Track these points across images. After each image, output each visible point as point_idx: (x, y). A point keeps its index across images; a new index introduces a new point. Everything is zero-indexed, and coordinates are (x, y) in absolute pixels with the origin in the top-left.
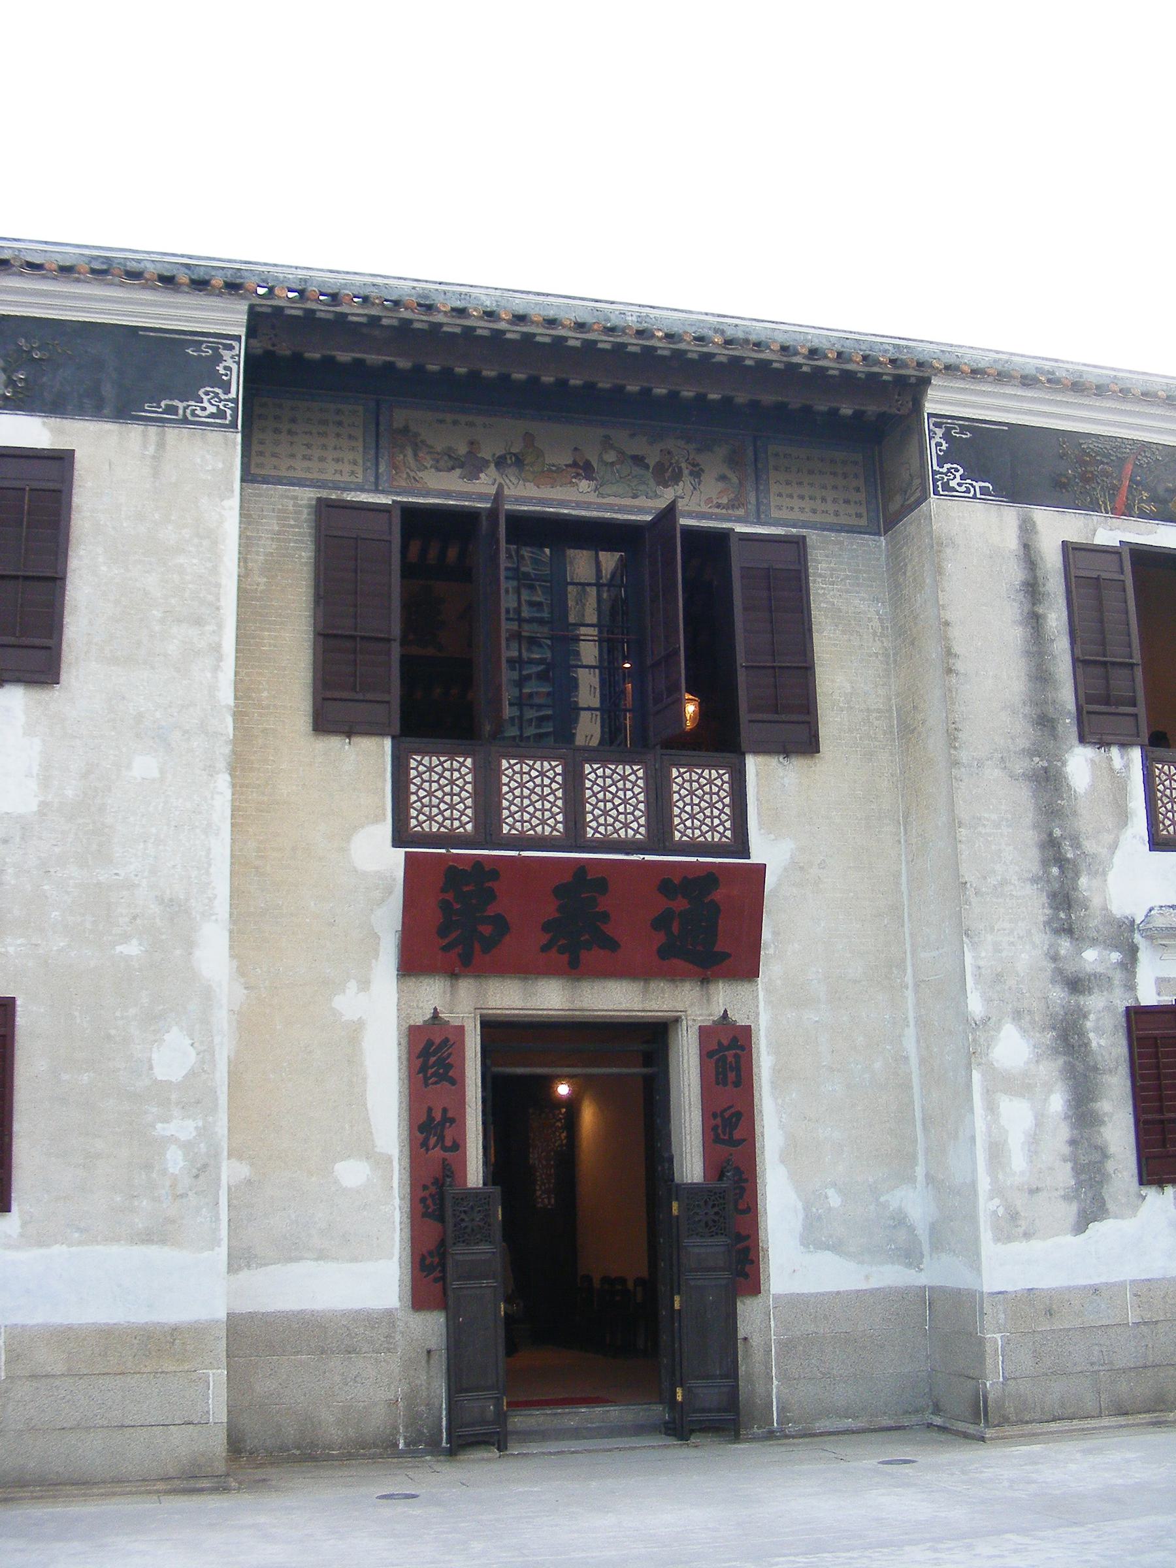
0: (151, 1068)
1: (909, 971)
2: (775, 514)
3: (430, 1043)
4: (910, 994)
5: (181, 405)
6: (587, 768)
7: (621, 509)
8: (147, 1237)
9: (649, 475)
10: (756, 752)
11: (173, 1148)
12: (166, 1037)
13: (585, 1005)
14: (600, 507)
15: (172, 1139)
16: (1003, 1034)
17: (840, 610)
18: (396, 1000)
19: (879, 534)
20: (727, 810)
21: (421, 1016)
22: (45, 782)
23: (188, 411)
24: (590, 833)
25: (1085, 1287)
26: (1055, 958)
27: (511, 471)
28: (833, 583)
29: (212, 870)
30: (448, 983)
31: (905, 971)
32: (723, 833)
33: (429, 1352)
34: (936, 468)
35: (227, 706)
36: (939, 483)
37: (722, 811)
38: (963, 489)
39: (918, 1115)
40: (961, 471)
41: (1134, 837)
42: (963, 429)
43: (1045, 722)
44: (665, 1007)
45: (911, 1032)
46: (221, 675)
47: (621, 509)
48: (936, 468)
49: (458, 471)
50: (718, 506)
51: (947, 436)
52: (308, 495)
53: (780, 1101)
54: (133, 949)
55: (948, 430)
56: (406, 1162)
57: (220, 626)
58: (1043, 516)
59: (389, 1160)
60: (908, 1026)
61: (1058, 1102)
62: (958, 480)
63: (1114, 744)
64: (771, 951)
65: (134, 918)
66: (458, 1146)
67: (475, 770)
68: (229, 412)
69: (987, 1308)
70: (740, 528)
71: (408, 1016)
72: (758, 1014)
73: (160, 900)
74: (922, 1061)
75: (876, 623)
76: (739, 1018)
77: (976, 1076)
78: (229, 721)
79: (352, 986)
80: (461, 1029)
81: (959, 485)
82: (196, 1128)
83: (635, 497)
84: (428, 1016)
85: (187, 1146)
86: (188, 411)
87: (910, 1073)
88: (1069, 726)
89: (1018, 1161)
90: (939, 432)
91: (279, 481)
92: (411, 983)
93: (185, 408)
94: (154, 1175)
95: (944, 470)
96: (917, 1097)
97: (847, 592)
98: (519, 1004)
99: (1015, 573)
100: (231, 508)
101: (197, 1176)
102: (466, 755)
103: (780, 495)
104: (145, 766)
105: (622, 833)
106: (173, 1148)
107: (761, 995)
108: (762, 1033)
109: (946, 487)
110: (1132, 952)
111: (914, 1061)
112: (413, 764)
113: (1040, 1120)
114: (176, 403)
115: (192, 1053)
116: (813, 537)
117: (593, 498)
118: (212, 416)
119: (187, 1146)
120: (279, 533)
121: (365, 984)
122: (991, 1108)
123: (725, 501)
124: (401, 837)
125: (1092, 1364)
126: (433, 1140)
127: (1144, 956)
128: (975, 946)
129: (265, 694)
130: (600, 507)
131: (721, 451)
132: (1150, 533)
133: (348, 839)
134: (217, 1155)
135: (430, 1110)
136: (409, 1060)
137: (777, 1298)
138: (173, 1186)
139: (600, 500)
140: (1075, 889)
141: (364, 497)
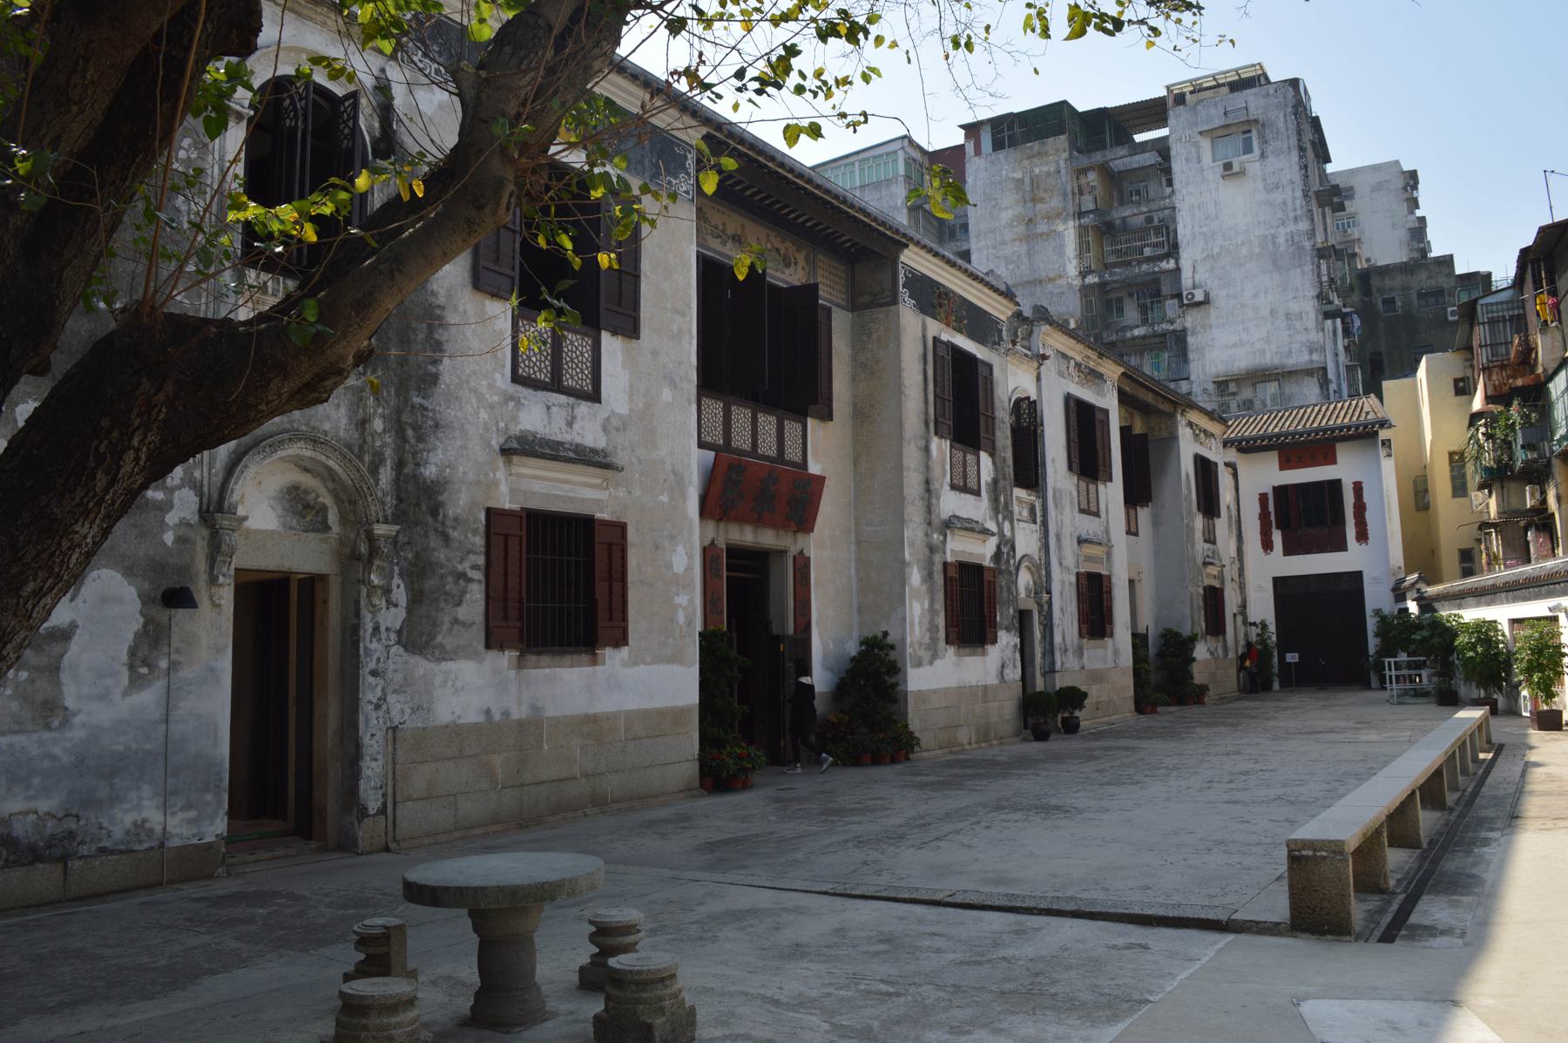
9: (781, 260)
10: (812, 417)
15: (680, 605)
21: (707, 543)
26: (927, 535)
27: (737, 244)
32: (798, 458)
42: (910, 272)
45: (853, 565)
51: (905, 274)
58: (929, 321)
85: (685, 609)
98: (738, 538)
99: (920, 350)
110: (945, 536)
116: (834, 308)
119: (685, 609)
122: (911, 605)
124: (702, 445)
127: (949, 538)
131: (803, 253)
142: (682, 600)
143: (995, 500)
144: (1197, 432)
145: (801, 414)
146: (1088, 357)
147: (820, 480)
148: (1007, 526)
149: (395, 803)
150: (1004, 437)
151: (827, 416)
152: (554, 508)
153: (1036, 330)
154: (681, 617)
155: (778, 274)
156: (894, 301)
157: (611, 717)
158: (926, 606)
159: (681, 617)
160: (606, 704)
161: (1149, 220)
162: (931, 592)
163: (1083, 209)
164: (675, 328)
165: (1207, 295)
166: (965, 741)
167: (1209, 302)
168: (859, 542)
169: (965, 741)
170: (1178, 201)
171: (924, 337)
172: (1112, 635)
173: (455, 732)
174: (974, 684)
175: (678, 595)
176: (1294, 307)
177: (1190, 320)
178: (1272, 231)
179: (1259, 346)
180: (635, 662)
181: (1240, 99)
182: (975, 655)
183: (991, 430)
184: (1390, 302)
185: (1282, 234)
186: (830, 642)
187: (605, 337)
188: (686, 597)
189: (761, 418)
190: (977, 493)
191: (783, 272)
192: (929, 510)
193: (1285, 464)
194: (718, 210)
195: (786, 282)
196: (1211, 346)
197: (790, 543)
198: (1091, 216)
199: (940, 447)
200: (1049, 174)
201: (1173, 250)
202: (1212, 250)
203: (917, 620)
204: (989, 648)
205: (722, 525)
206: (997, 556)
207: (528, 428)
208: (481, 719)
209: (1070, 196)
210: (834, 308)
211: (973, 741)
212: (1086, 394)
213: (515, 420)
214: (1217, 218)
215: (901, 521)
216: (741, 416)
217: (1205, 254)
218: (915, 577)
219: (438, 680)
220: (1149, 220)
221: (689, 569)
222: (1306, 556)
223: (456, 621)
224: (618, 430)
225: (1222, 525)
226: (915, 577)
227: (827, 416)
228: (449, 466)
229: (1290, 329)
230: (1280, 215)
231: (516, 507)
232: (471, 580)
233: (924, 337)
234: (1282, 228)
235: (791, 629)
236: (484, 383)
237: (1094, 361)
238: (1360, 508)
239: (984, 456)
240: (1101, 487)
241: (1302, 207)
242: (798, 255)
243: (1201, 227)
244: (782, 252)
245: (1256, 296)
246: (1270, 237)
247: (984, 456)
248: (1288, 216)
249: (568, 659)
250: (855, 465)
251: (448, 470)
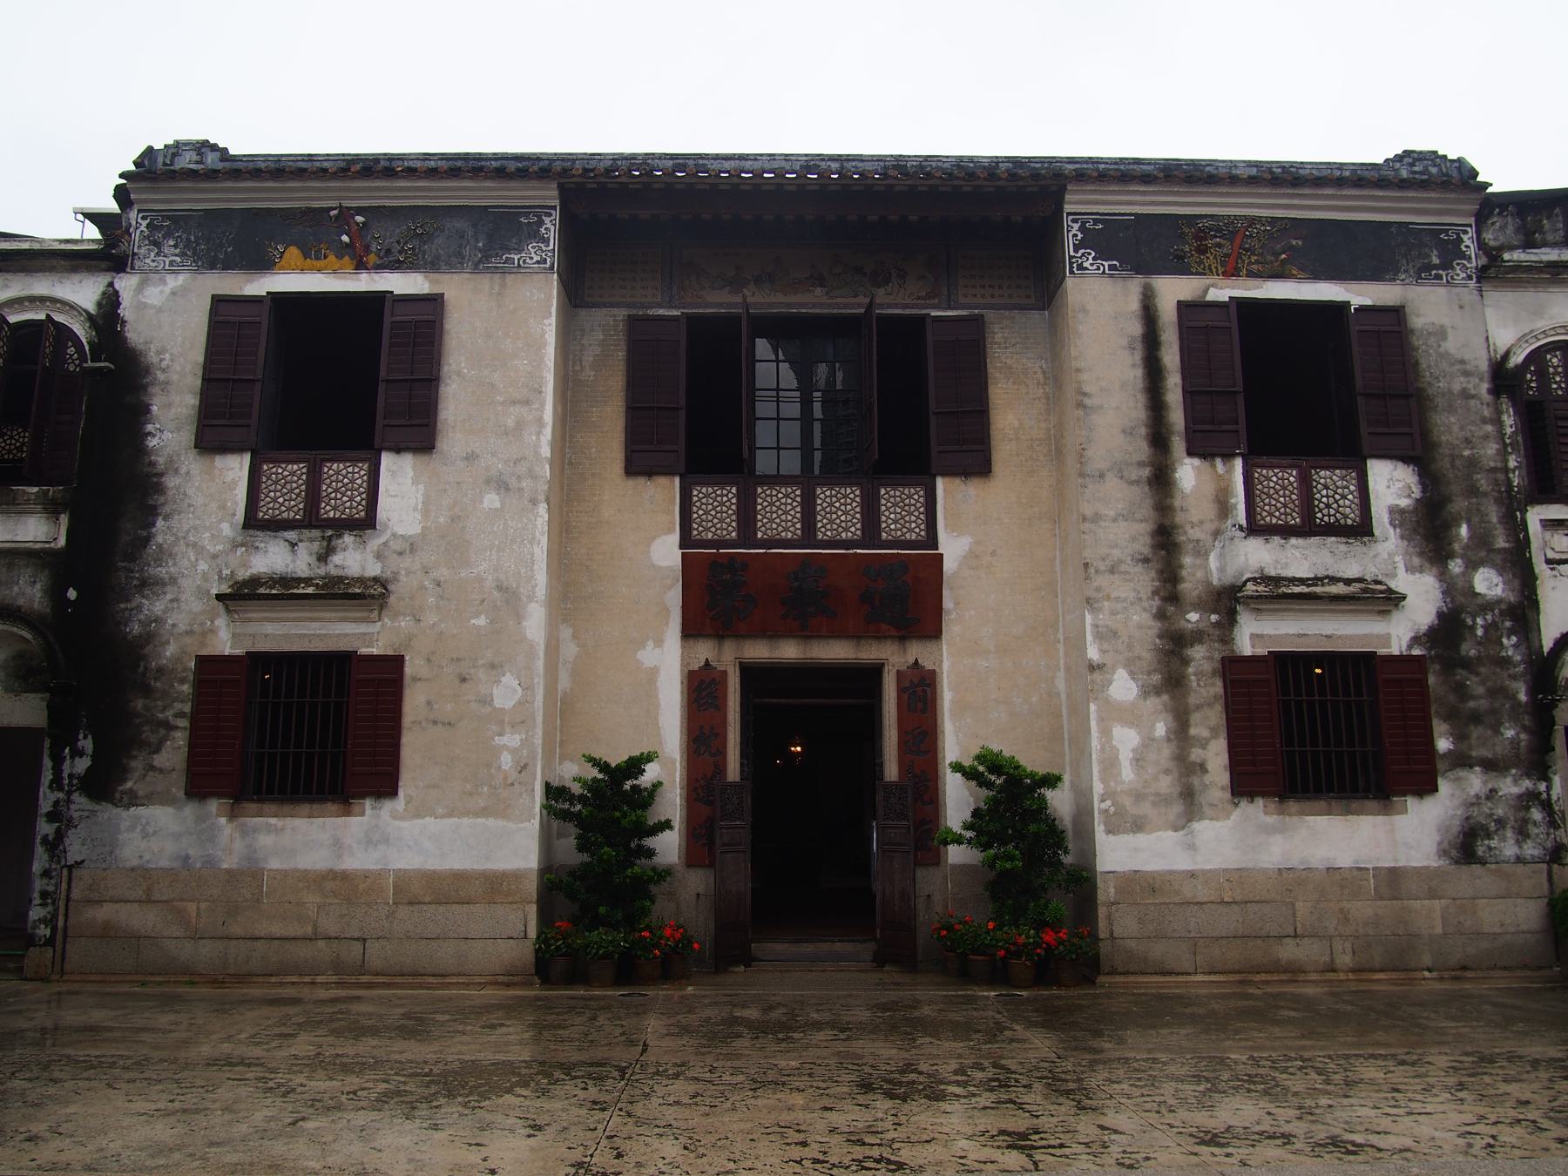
0: (492, 700)
1: (1061, 630)
2: (962, 300)
3: (702, 682)
4: (1061, 647)
5: (516, 257)
6: (819, 491)
7: (846, 306)
8: (484, 812)
10: (943, 475)
11: (505, 753)
12: (503, 679)
13: (814, 656)
14: (830, 306)
15: (505, 747)
16: (1116, 677)
17: (1011, 368)
18: (680, 654)
19: (1044, 309)
20: (922, 516)
22: (426, 513)
23: (521, 262)
24: (820, 536)
25: (1183, 871)
26: (1161, 615)
28: (1006, 348)
29: (535, 567)
30: (716, 641)
31: (1058, 631)
32: (917, 532)
33: (698, 895)
34: (1072, 253)
35: (546, 458)
36: (1075, 265)
37: (918, 518)
38: (1095, 267)
39: (1066, 736)
40: (1093, 254)
41: (1235, 526)
42: (1096, 222)
43: (1159, 439)
44: (872, 657)
45: (1061, 674)
46: (542, 437)
47: (846, 306)
48: (1072, 253)
50: (918, 298)
52: (622, 313)
53: (957, 724)
54: (481, 621)
55: (1084, 223)
56: (685, 764)
57: (543, 405)
59: (674, 762)
60: (1059, 670)
61: (1161, 730)
62: (1091, 261)
63: (1218, 455)
64: (953, 617)
65: (483, 601)
66: (722, 753)
67: (738, 495)
68: (548, 259)
69: (1100, 883)
70: (934, 313)
71: (688, 664)
72: (942, 662)
73: (500, 588)
74: (1068, 696)
75: (1040, 376)
76: (928, 664)
77: (1093, 707)
78: (547, 467)
79: (650, 644)
80: (725, 672)
81: (1092, 265)
82: (521, 740)
83: (855, 296)
84: (702, 664)
85: (513, 751)
86: (521, 262)
87: (1061, 705)
88: (1178, 445)
89: (1127, 773)
90: (1076, 226)
91: (605, 305)
92: (691, 642)
93: (519, 260)
94: (493, 771)
95: (1079, 255)
96: (1065, 722)
97: (1017, 353)
98: (767, 655)
99: (1136, 329)
100: (550, 325)
101: (520, 772)
102: (731, 484)
103: (966, 286)
104: (492, 500)
105: (844, 535)
106: (505, 753)
107: (944, 647)
108: (945, 675)
109: (1080, 267)
111: (1063, 697)
112: (695, 493)
113: (1148, 741)
114: (512, 256)
115: (519, 690)
116: (989, 315)
117: (825, 300)
118: (538, 262)
119: (513, 751)
120: (603, 340)
121: (659, 643)
122: (1106, 732)
123: (923, 294)
125: (1189, 932)
128: (1094, 610)
129: (594, 450)
130: (830, 306)
132: (1258, 288)
133: (649, 546)
134: (534, 758)
135: (702, 727)
136: (688, 694)
137: (954, 867)
138: (505, 778)
139: (830, 301)
140: (1181, 567)
141: (661, 312)
149: (65, 936)
152: (295, 648)
160: (358, 860)
164: (510, 422)
173: (142, 873)
175: (500, 735)
188: (517, 737)
197: (894, 658)
207: (262, 570)
208: (176, 864)
210: (989, 315)
213: (246, 566)
219: (124, 825)
223: (152, 768)
224: (400, 554)
228: (155, 621)
231: (238, 652)
232: (177, 728)
236: (207, 535)
251: (153, 625)
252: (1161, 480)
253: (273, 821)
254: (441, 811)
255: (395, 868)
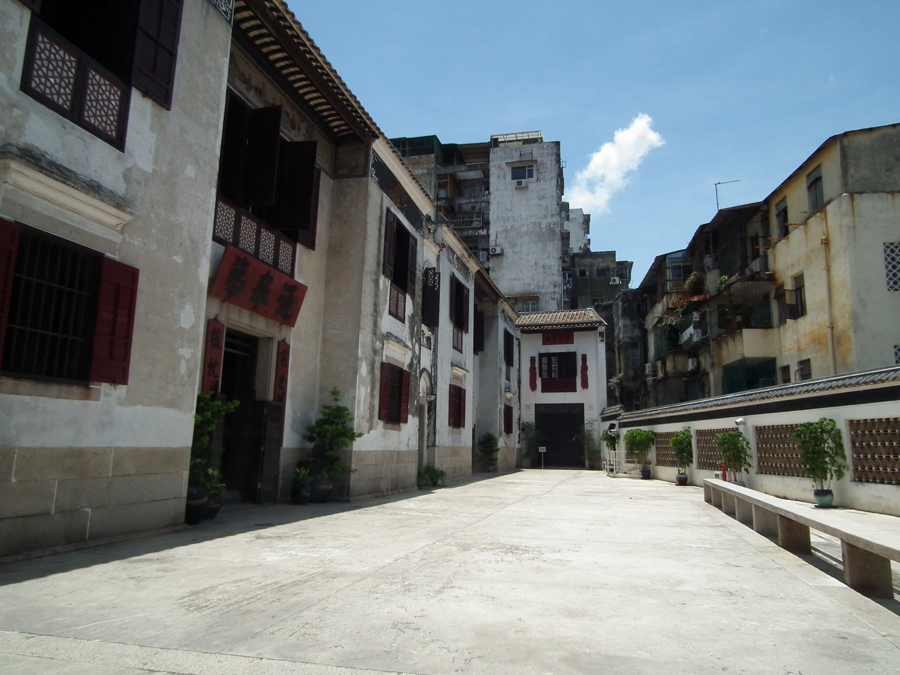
10: (300, 243)
15: (183, 357)
21: (212, 317)
43: (378, 264)
45: (319, 357)
49: (245, 85)
51: (374, 158)
55: (374, 156)
85: (188, 361)
110: (383, 344)
119: (188, 361)
124: (215, 238)
126: (211, 372)
142: (185, 352)
143: (412, 328)
144: (506, 316)
145: (293, 240)
146: (463, 255)
147: (304, 288)
148: (417, 346)
150: (418, 287)
151: (310, 244)
153: (439, 229)
154: (183, 368)
155: (286, 131)
156: (365, 174)
157: (97, 453)
158: (369, 391)
159: (183, 368)
160: (92, 440)
161: (474, 208)
162: (373, 382)
163: (439, 197)
165: (502, 250)
166: (385, 489)
167: (503, 255)
168: (324, 341)
169: (385, 489)
170: (493, 199)
171: (382, 205)
172: (464, 426)
174: (392, 449)
175: (182, 348)
176: (548, 262)
177: (491, 264)
178: (539, 220)
179: (528, 281)
180: (130, 401)
181: (528, 148)
182: (394, 430)
183: (413, 283)
184: (583, 273)
185: (544, 223)
186: (298, 411)
187: (136, 97)
188: (190, 351)
189: (264, 233)
190: (403, 321)
191: (290, 132)
192: (375, 324)
193: (546, 342)
194: (246, 62)
195: (290, 138)
196: (502, 278)
198: (444, 201)
199: (385, 283)
200: (423, 175)
201: (486, 224)
202: (507, 227)
203: (362, 400)
204: (402, 425)
205: (225, 305)
206: (411, 365)
209: (433, 188)
211: (389, 489)
212: (460, 277)
214: (511, 210)
215: (358, 327)
216: (249, 227)
217: (503, 229)
218: (364, 369)
220: (474, 208)
221: (194, 327)
222: (554, 393)
225: (514, 371)
226: (364, 369)
227: (310, 244)
229: (544, 274)
230: (544, 212)
233: (382, 205)
234: (544, 220)
235: (271, 397)
237: (466, 259)
238: (585, 368)
239: (408, 297)
240: (464, 335)
241: (555, 209)
242: (301, 124)
243: (502, 214)
244: (291, 116)
245: (528, 254)
246: (538, 224)
247: (408, 297)
248: (548, 213)
249: (55, 389)
250: (326, 286)
252: (377, 282)
253: (27, 398)
254: (146, 400)
255: (116, 446)
